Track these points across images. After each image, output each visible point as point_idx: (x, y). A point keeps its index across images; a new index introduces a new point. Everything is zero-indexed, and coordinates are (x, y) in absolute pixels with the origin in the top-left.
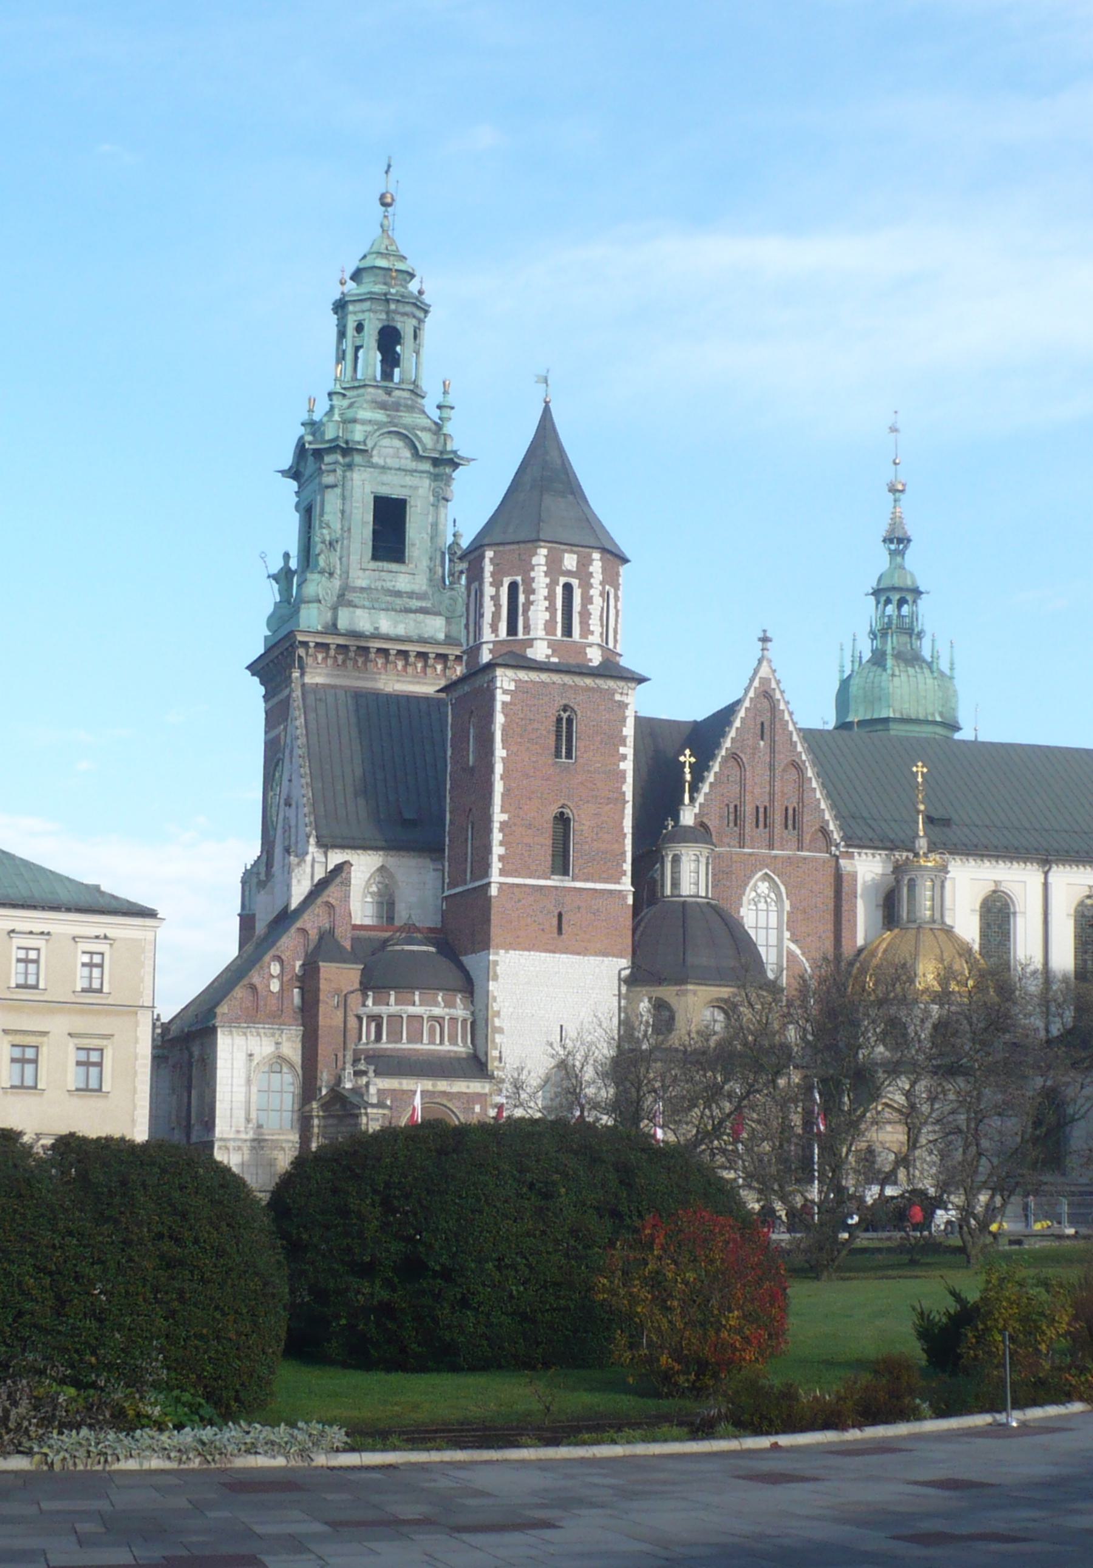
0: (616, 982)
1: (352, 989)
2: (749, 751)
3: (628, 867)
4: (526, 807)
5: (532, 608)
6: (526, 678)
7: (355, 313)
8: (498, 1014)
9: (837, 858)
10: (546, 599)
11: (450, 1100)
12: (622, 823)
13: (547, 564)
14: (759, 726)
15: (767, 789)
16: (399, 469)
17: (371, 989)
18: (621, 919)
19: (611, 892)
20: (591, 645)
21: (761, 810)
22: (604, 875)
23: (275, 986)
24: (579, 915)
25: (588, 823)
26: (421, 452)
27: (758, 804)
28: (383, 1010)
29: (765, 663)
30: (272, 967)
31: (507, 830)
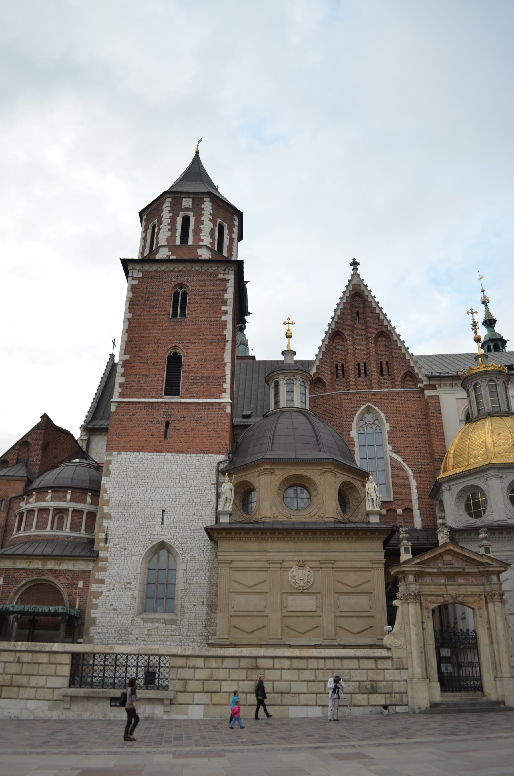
1: (17, 495)
2: (348, 328)
3: (227, 386)
4: (144, 349)
5: (161, 232)
6: (151, 270)
9: (422, 390)
10: (169, 224)
11: (57, 577)
13: (171, 206)
15: (365, 352)
19: (212, 403)
20: (201, 247)
21: (362, 365)
22: (207, 393)
25: (195, 358)
27: (359, 361)
29: (356, 277)
31: (128, 366)
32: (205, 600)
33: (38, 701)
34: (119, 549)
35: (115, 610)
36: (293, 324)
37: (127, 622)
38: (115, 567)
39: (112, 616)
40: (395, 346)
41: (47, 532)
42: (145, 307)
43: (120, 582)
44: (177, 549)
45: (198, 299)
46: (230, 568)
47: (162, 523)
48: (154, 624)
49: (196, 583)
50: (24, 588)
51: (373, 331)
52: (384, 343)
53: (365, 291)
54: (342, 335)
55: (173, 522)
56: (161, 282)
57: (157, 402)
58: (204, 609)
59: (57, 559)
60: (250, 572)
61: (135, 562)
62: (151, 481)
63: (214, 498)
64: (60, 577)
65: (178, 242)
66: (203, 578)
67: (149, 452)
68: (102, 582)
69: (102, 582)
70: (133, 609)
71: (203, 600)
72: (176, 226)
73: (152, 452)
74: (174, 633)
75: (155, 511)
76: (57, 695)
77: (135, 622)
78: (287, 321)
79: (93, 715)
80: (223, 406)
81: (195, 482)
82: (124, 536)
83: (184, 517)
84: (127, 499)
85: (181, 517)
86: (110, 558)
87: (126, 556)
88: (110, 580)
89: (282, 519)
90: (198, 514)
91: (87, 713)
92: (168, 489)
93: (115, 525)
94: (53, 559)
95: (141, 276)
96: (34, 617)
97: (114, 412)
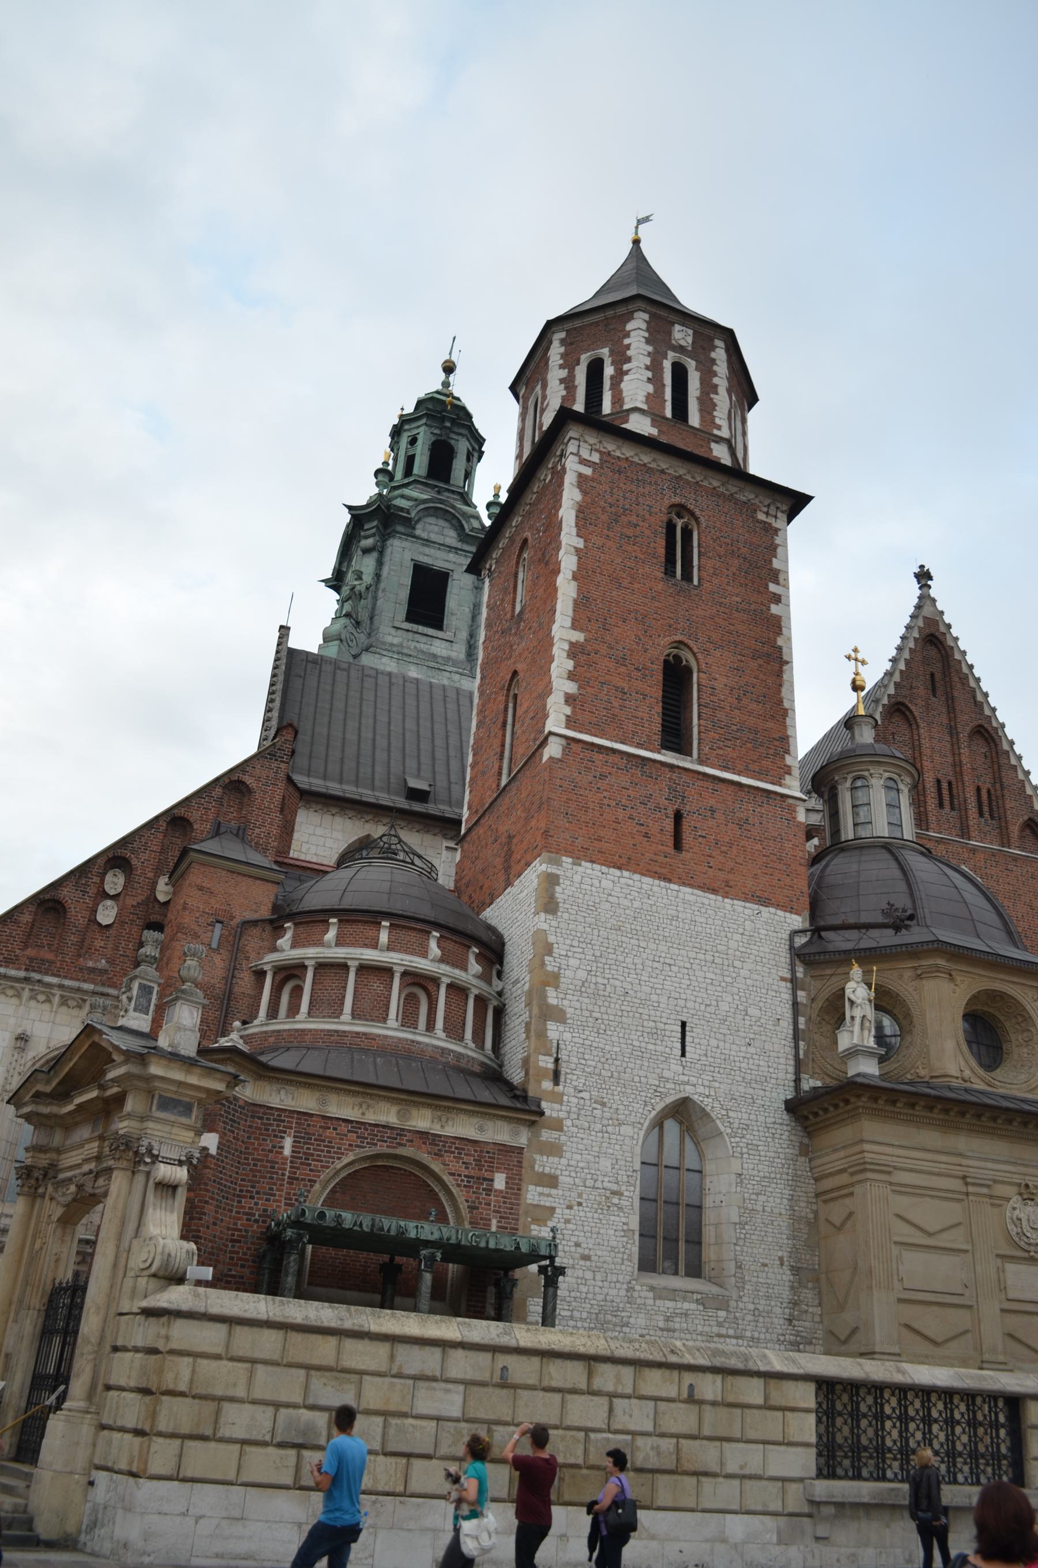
0: (784, 957)
1: (255, 916)
5: (626, 378)
6: (618, 454)
7: (409, 430)
8: (554, 979)
10: (647, 368)
12: (780, 692)
13: (648, 330)
14: (928, 677)
15: (950, 759)
16: (443, 545)
17: (290, 917)
18: (788, 845)
20: (719, 440)
21: (945, 785)
23: (107, 914)
24: (711, 823)
26: (467, 531)
28: (310, 953)
30: (109, 877)
31: (583, 658)
32: (785, 1254)
33: (746, 1516)
34: (588, 1103)
35: (586, 1258)
36: (863, 663)
37: (617, 1293)
38: (580, 1146)
39: (580, 1273)
40: (1006, 761)
41: (391, 1029)
42: (611, 534)
43: (593, 1187)
44: (718, 1122)
45: (722, 550)
46: (891, 1184)
47: (683, 1055)
48: (679, 1305)
49: (764, 1211)
50: (343, 1174)
51: (966, 723)
52: (984, 750)
53: (948, 636)
54: (907, 713)
55: (706, 1055)
56: (641, 489)
57: (655, 761)
58: (785, 1277)
59: (437, 1107)
60: (927, 1199)
61: (627, 1141)
62: (654, 946)
63: (788, 1014)
64: (448, 1158)
65: (668, 413)
66: (778, 1201)
67: (643, 874)
68: (551, 1181)
69: (551, 1181)
70: (630, 1261)
71: (780, 1254)
72: (662, 378)
73: (650, 876)
74: (723, 1331)
75: (664, 1020)
76: (794, 1500)
77: (636, 1294)
78: (853, 655)
79: (884, 1556)
80: (790, 805)
81: (747, 966)
82: (597, 1071)
83: (727, 1045)
84: (600, 980)
85: (721, 1044)
86: (569, 1123)
87: (605, 1122)
88: (568, 1179)
89: (980, 1086)
90: (757, 1043)
91: (871, 1551)
92: (691, 972)
93: (576, 1040)
94: (429, 1106)
95: (598, 461)
96: (392, 1260)
97: (560, 760)
